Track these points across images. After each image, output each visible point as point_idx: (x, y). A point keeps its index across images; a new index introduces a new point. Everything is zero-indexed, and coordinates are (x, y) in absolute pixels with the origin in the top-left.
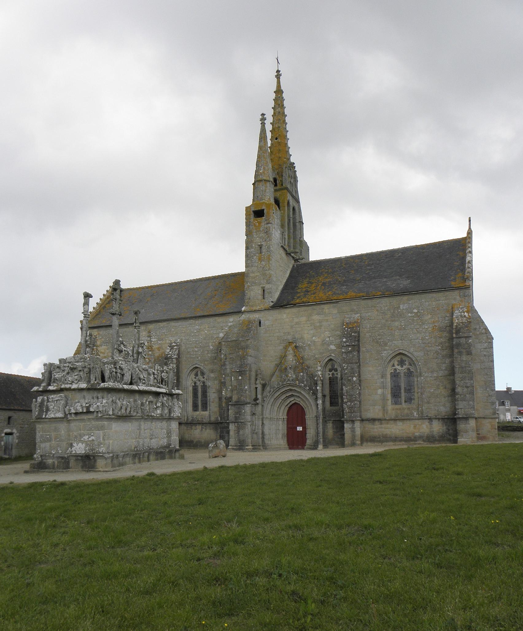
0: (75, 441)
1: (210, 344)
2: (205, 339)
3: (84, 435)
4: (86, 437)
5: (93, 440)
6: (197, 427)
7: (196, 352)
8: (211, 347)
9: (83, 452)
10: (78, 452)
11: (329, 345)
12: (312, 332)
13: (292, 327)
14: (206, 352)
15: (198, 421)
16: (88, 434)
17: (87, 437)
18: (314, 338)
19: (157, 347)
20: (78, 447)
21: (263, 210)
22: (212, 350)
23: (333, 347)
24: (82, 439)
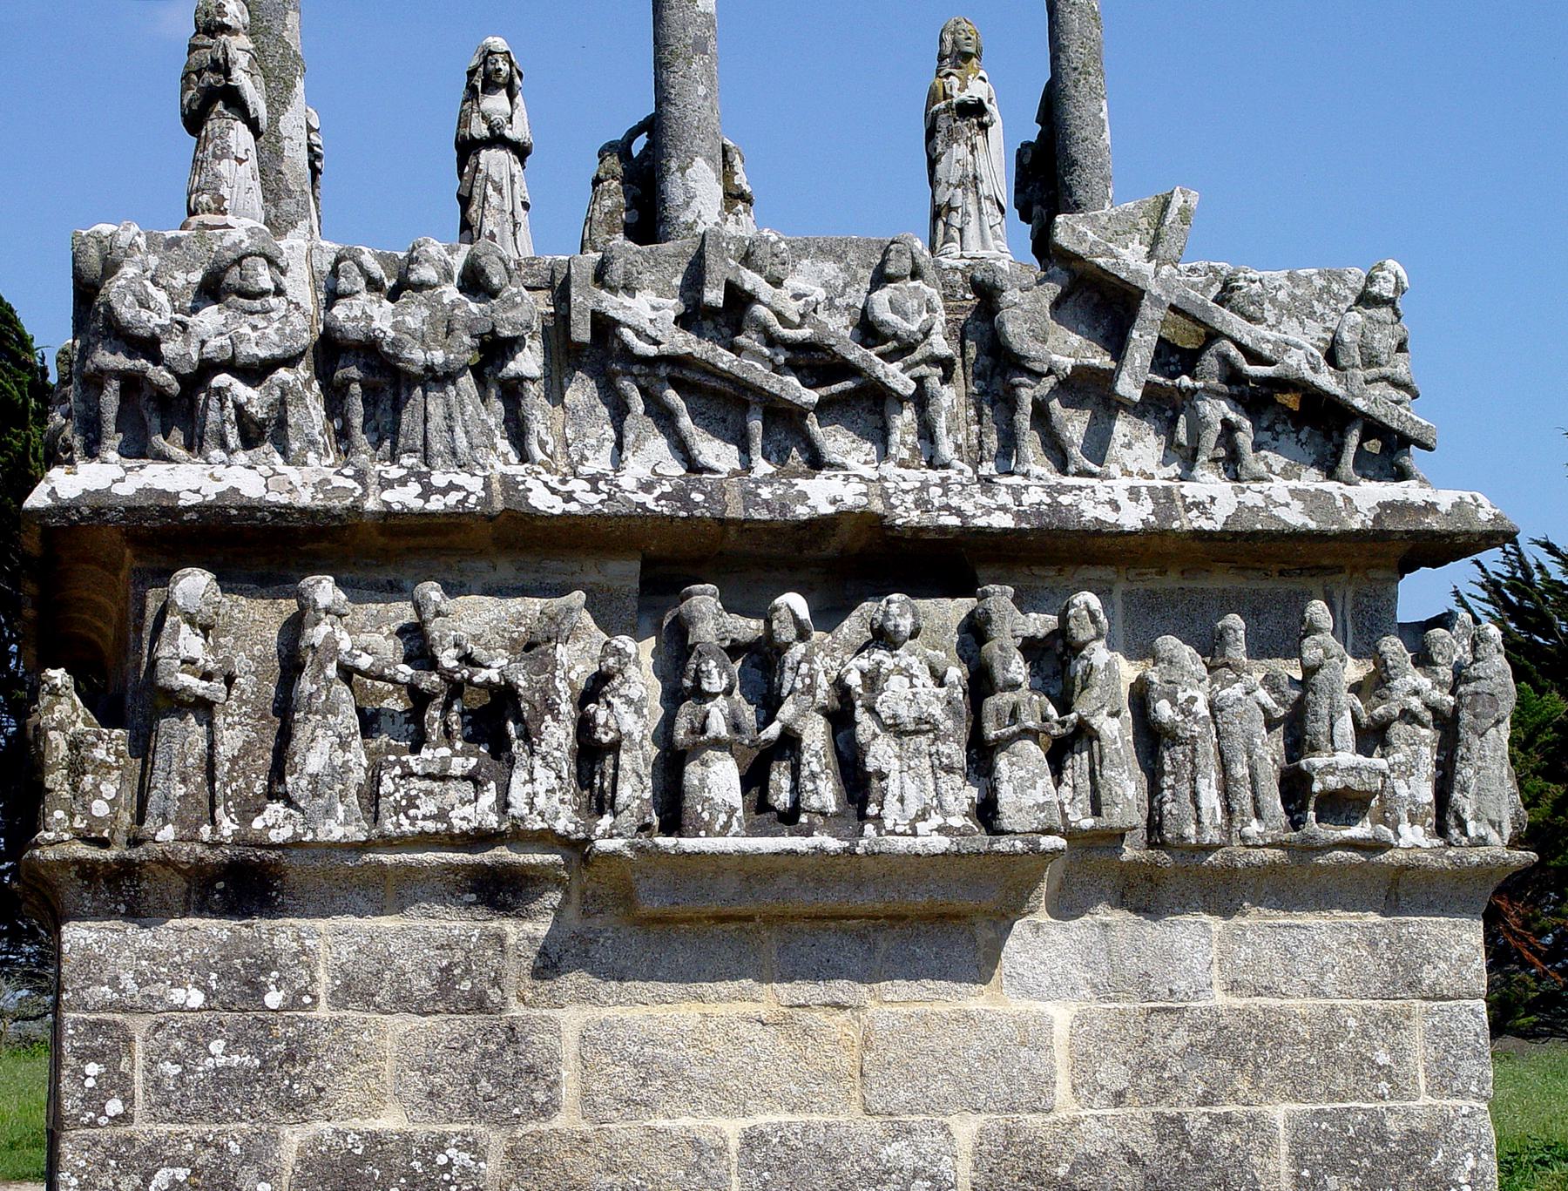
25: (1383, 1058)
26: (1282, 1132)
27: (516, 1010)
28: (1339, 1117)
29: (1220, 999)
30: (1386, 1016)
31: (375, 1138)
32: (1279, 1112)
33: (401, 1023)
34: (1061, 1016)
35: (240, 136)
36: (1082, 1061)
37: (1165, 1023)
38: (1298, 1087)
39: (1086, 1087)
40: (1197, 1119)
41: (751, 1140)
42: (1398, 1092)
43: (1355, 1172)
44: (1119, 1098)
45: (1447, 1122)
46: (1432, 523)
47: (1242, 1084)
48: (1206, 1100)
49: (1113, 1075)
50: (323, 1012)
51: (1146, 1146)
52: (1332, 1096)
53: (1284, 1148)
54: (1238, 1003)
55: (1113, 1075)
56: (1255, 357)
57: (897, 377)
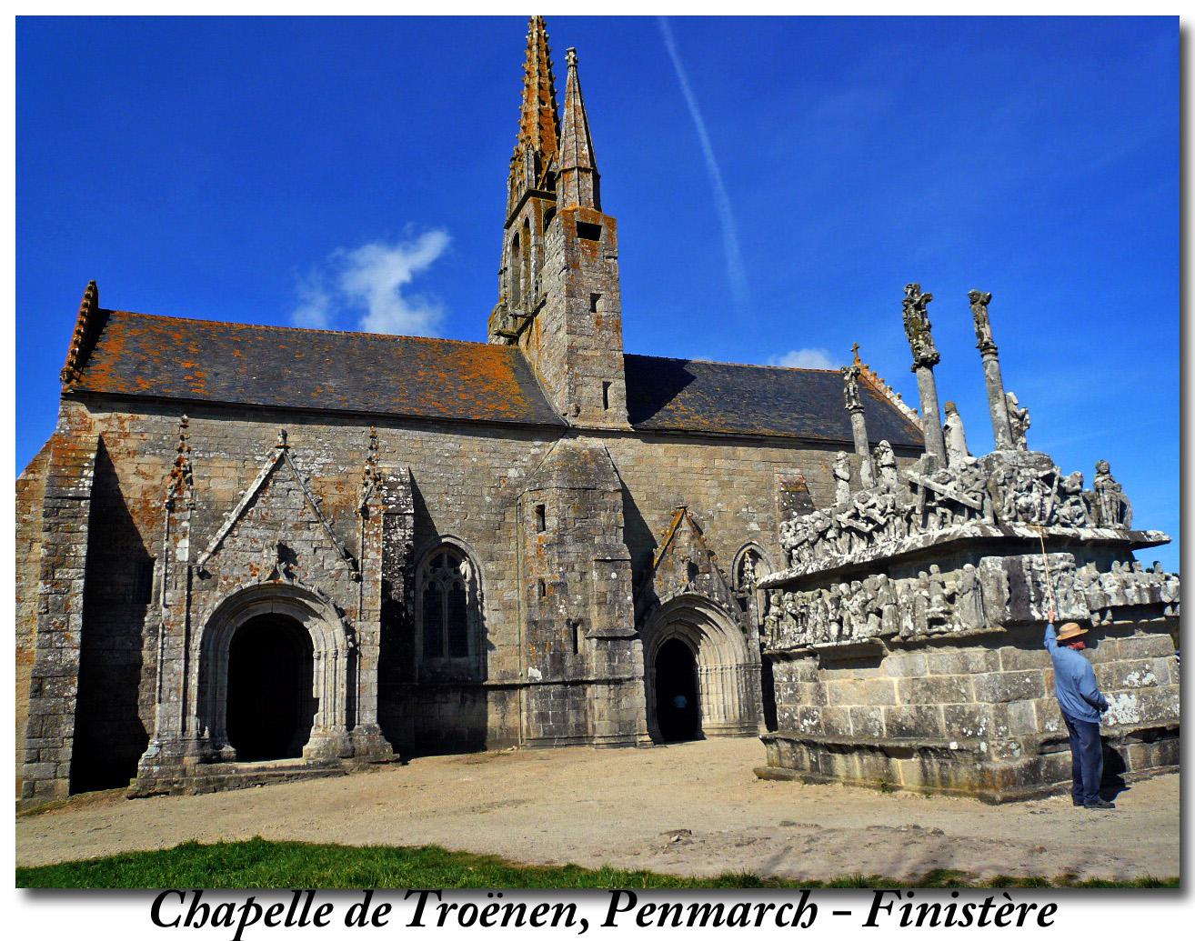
0: (1106, 688)
1: (485, 491)
2: (472, 476)
3: (1129, 670)
4: (1134, 677)
5: (1153, 684)
6: (451, 696)
7: (448, 506)
8: (488, 499)
9: (1136, 719)
10: (1122, 722)
11: (747, 522)
12: (714, 492)
13: (674, 475)
14: (475, 509)
15: (452, 679)
16: (1140, 668)
17: (1137, 675)
18: (719, 505)
19: (334, 478)
20: (1119, 706)
21: (600, 227)
22: (490, 506)
23: (754, 526)
24: (1126, 682)
25: (963, 691)
26: (942, 712)
27: (821, 681)
28: (954, 707)
29: (928, 675)
30: (963, 679)
31: (807, 708)
32: (942, 706)
33: (808, 684)
34: (895, 680)
35: (841, 483)
36: (901, 692)
37: (916, 682)
38: (944, 698)
39: (903, 699)
40: (924, 707)
41: (851, 711)
42: (968, 700)
43: (958, 722)
44: (909, 702)
45: (979, 709)
46: (946, 539)
47: (933, 699)
48: (926, 703)
49: (908, 697)
50: (799, 682)
51: (915, 714)
52: (953, 701)
53: (943, 715)
54: (932, 676)
55: (908, 697)
56: (941, 495)
57: (882, 520)
